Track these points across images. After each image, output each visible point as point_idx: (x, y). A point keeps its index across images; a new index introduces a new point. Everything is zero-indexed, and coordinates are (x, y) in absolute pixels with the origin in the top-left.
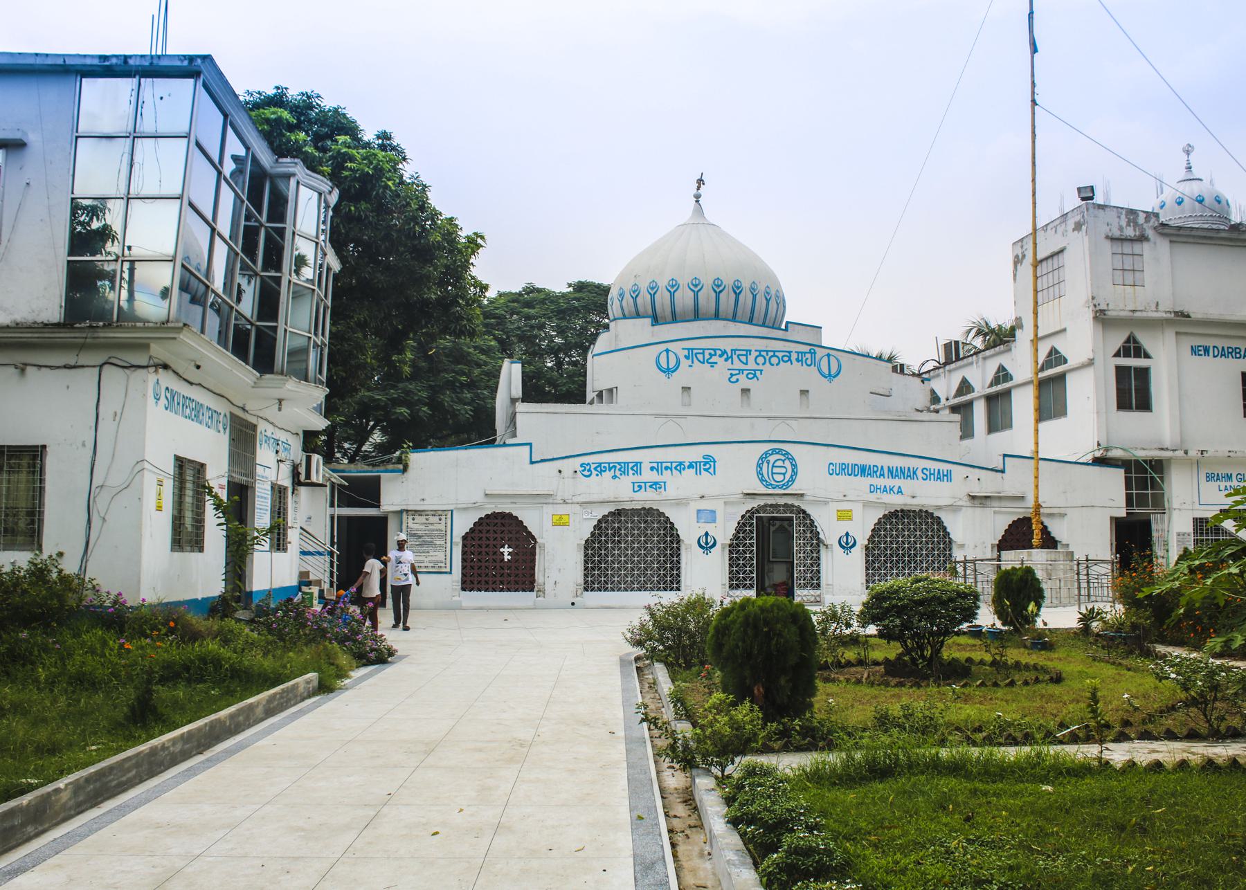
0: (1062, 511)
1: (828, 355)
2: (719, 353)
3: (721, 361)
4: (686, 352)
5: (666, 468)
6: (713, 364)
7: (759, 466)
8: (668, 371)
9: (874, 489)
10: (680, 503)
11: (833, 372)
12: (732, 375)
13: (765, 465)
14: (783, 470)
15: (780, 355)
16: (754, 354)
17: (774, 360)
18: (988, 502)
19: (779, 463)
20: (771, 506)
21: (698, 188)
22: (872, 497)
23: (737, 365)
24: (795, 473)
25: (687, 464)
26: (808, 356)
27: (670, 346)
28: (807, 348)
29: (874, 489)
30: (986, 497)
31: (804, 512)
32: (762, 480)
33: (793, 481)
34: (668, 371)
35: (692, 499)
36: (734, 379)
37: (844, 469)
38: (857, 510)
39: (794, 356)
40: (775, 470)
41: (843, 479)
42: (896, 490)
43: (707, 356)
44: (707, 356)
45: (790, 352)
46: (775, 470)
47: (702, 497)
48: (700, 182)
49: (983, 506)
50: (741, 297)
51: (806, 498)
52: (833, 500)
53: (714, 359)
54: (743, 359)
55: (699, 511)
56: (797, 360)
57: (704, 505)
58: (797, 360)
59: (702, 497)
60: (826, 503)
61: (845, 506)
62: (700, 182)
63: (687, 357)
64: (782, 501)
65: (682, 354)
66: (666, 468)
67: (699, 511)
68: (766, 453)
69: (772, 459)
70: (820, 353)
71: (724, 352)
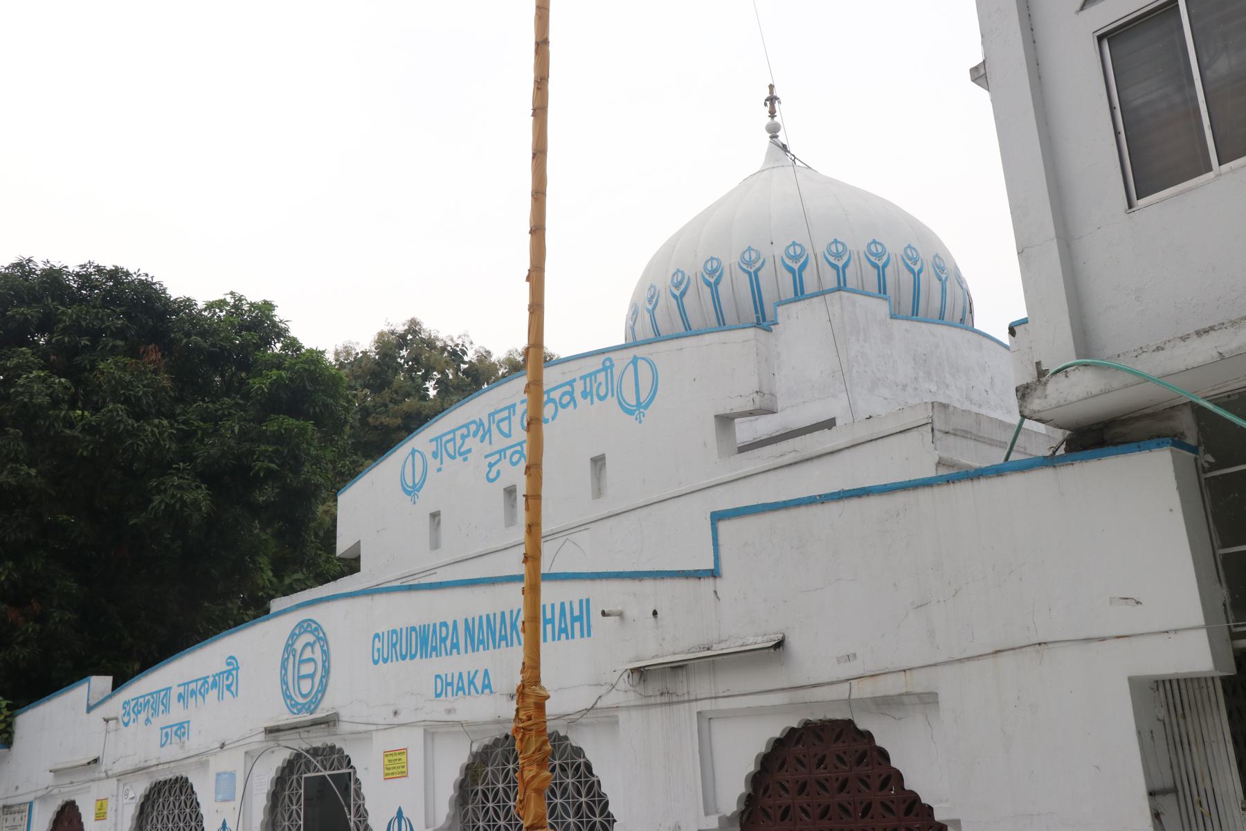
0: (919, 683)
2: (473, 428)
4: (433, 447)
5: (193, 693)
6: (465, 454)
12: (491, 465)
15: (555, 395)
18: (681, 686)
20: (315, 752)
26: (601, 377)
30: (677, 668)
36: (492, 475)
42: (479, 682)
45: (571, 383)
48: (772, 100)
49: (670, 699)
50: (721, 288)
51: (344, 727)
55: (218, 775)
56: (585, 395)
58: (585, 395)
62: (772, 100)
67: (218, 775)
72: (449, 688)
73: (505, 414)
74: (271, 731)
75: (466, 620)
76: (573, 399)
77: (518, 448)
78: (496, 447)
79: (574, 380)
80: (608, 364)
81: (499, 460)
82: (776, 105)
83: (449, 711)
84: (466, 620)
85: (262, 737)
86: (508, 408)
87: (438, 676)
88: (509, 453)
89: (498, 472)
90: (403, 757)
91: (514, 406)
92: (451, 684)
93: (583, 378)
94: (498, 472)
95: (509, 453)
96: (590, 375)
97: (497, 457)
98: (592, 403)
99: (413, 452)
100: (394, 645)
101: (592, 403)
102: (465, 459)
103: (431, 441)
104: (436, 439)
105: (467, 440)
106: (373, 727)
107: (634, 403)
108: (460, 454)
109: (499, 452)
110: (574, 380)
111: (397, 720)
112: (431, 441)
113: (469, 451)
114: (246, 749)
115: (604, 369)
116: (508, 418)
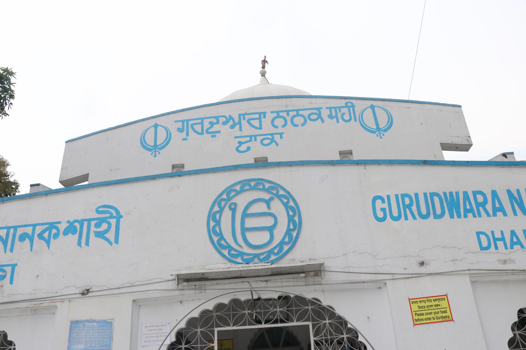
1: (373, 107)
3: (225, 129)
4: (180, 125)
6: (214, 135)
7: (214, 217)
8: (155, 149)
9: (489, 242)
10: (39, 307)
11: (383, 124)
12: (240, 143)
13: (227, 214)
14: (268, 222)
15: (306, 113)
16: (270, 116)
17: (299, 120)
19: (261, 207)
21: (263, 67)
22: (490, 260)
23: (247, 130)
24: (296, 225)
25: (62, 227)
26: (345, 110)
27: (158, 121)
28: (343, 103)
29: (489, 242)
31: (330, 313)
32: (219, 245)
33: (293, 242)
34: (155, 149)
35: (68, 299)
37: (407, 207)
38: (460, 295)
39: (325, 113)
40: (250, 223)
41: (409, 226)
43: (206, 125)
44: (206, 125)
45: (319, 109)
46: (250, 223)
47: (86, 293)
48: (264, 62)
51: (329, 277)
52: (394, 277)
53: (215, 128)
54: (256, 123)
55: (74, 324)
57: (88, 310)
58: (330, 117)
59: (86, 293)
60: (379, 285)
61: (428, 288)
62: (264, 62)
63: (180, 130)
64: (271, 290)
65: (173, 128)
66: (22, 238)
67: (74, 324)
68: (229, 190)
69: (242, 201)
70: (359, 106)
71: (231, 118)
72: (500, 244)
73: (257, 116)
74: (188, 280)
75: (509, 192)
76: (320, 117)
77: (270, 137)
78: (244, 133)
79: (322, 108)
80: (350, 105)
81: (250, 141)
82: (266, 64)
83: (505, 262)
84: (509, 192)
85: (173, 285)
86: (260, 114)
87: (478, 234)
88: (259, 139)
89: (249, 149)
90: (444, 304)
91: (265, 114)
92: (503, 239)
93: (330, 109)
94: (249, 149)
95: (259, 139)
96: (335, 108)
97: (248, 139)
98: (338, 122)
99: (156, 126)
100: (409, 206)
101: (338, 122)
102: (215, 136)
103: (175, 122)
104: (183, 121)
105: (215, 126)
106: (390, 277)
107: (375, 128)
108: (208, 132)
109: (251, 137)
110: (322, 108)
111: (423, 270)
112: (175, 122)
113: (219, 132)
114: (136, 297)
115: (346, 106)
116: (260, 119)
